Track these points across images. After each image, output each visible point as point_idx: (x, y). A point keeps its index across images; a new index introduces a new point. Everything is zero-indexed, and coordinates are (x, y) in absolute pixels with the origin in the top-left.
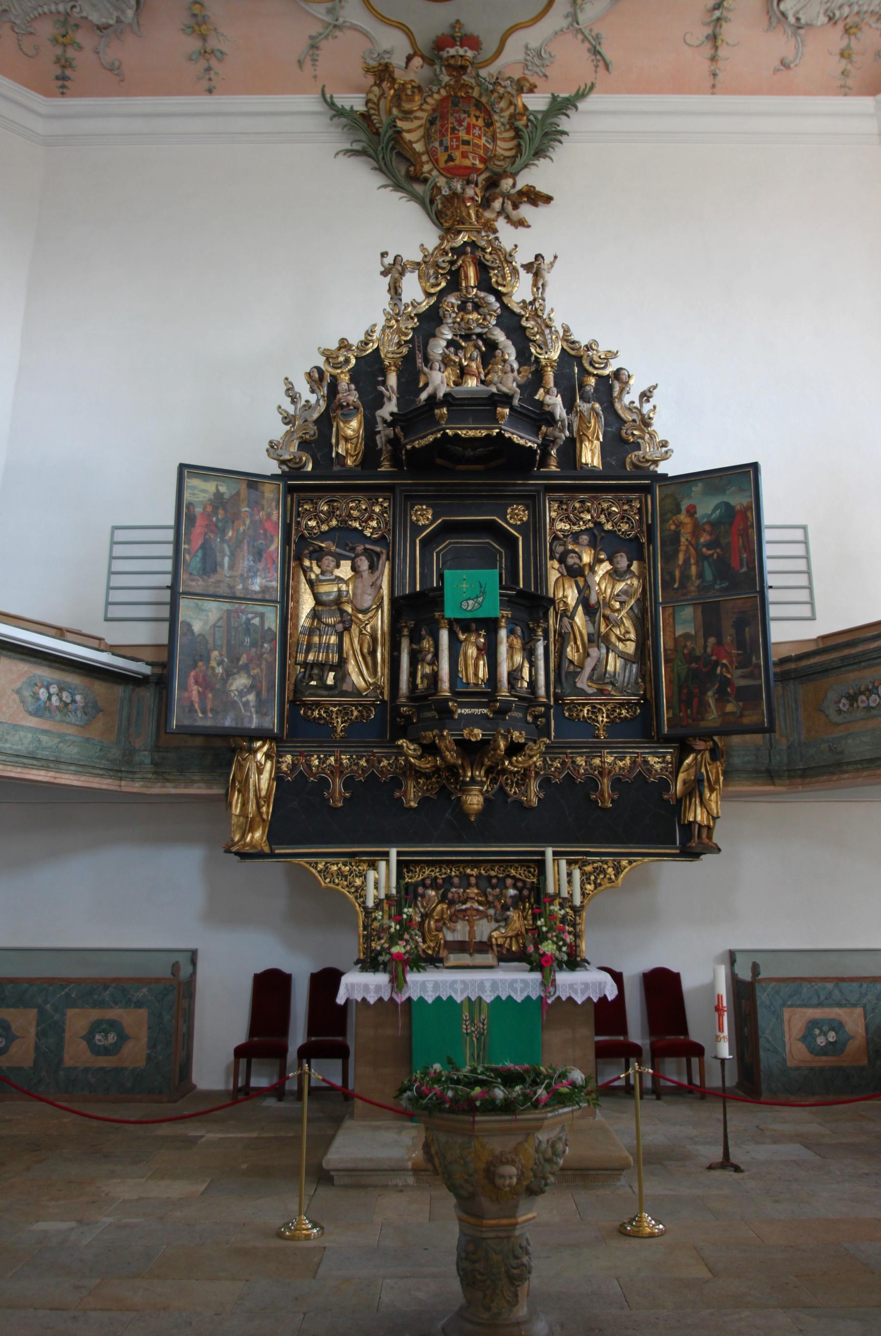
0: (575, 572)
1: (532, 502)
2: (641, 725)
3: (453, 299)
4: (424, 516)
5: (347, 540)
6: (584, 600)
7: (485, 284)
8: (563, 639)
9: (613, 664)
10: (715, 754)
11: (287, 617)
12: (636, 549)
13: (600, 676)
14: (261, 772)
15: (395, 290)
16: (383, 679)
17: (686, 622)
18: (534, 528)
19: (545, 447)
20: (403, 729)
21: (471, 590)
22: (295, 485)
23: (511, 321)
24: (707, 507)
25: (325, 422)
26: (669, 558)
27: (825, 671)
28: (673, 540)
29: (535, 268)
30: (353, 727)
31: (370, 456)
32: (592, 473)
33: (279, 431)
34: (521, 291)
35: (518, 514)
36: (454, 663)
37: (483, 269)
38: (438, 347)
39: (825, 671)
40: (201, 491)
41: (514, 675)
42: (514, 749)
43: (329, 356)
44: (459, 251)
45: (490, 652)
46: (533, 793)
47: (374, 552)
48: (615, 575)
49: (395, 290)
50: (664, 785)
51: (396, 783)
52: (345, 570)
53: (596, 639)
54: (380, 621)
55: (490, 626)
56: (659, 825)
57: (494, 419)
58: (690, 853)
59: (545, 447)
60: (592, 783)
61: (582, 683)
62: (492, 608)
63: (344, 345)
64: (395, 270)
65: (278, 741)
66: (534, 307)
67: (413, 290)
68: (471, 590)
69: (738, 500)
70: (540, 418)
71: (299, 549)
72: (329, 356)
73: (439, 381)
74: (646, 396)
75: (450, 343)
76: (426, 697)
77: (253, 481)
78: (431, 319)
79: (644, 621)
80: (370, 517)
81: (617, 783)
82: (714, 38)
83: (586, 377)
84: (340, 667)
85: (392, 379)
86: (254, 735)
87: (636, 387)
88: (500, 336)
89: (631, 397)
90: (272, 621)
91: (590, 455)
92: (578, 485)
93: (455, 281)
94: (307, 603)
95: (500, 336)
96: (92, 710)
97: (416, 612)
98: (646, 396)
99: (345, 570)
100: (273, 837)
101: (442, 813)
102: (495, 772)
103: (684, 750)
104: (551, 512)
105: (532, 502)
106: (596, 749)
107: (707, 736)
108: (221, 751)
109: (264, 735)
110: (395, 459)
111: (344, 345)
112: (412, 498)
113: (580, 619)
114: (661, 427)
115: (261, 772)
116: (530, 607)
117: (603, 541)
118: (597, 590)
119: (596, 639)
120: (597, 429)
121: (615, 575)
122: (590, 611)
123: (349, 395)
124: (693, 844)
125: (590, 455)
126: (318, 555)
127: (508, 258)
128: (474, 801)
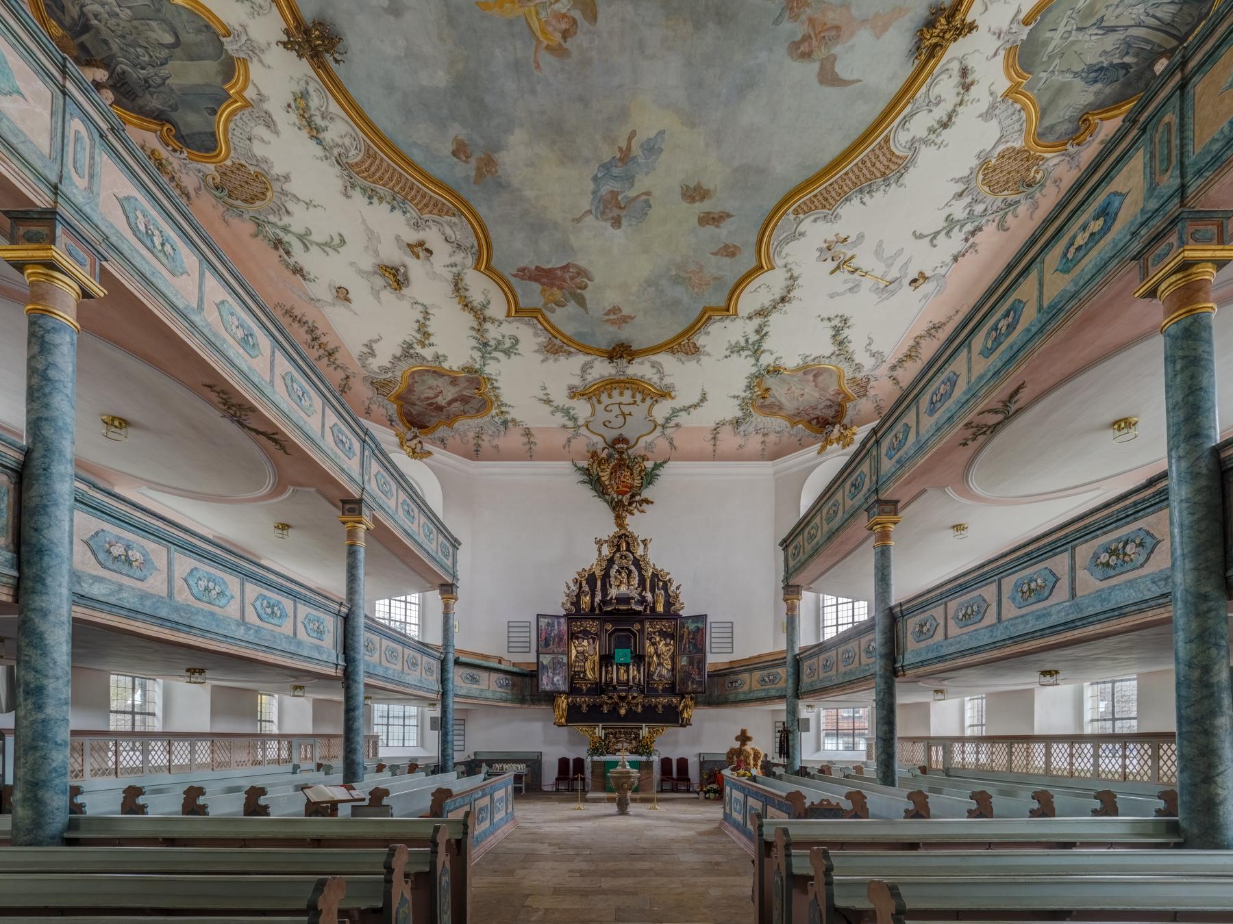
0: (654, 644)
1: (641, 622)
2: (671, 690)
3: (618, 555)
4: (609, 627)
5: (586, 634)
6: (656, 652)
7: (628, 549)
8: (650, 664)
9: (664, 672)
10: (692, 699)
11: (569, 657)
12: (672, 636)
13: (660, 675)
14: (563, 702)
15: (600, 551)
16: (597, 675)
17: (684, 661)
18: (641, 631)
19: (645, 609)
20: (603, 691)
21: (622, 655)
22: (569, 617)
23: (636, 562)
24: (692, 627)
25: (578, 596)
26: (681, 641)
27: (725, 675)
28: (682, 636)
29: (644, 541)
30: (588, 690)
31: (592, 608)
32: (660, 614)
33: (564, 599)
34: (640, 551)
35: (637, 626)
36: (616, 674)
37: (628, 544)
38: (613, 572)
39: (725, 675)
40: (543, 622)
41: (634, 678)
42: (634, 698)
43: (578, 574)
44: (620, 537)
45: (627, 671)
46: (640, 710)
47: (593, 637)
48: (666, 645)
49: (600, 551)
50: (677, 707)
51: (601, 706)
52: (585, 643)
53: (660, 664)
54: (597, 658)
55: (628, 665)
56: (673, 717)
57: (629, 603)
58: (682, 726)
59: (645, 609)
60: (656, 706)
61: (655, 677)
62: (629, 660)
63: (584, 570)
64: (599, 543)
65: (568, 694)
66: (644, 557)
67: (606, 551)
68: (622, 655)
69: (700, 626)
70: (643, 601)
71: (573, 636)
72: (578, 574)
73: (613, 592)
74: (678, 588)
75: (618, 571)
76: (609, 684)
77: (558, 617)
78: (611, 561)
79: (673, 658)
80: (593, 626)
81: (663, 706)
82: (714, 438)
83: (658, 581)
84: (585, 672)
85: (599, 583)
86: (560, 693)
87: (675, 585)
88: (632, 568)
89: (673, 588)
90: (565, 660)
91: (660, 608)
92: (655, 617)
93: (618, 550)
94: (574, 652)
95: (632, 568)
96: (514, 685)
97: (606, 660)
98: (678, 588)
99: (585, 643)
100: (567, 721)
101: (613, 714)
102: (628, 703)
103: (683, 697)
104: (647, 625)
105: (641, 622)
106: (657, 696)
107: (689, 693)
108: (550, 698)
109: (564, 692)
110: (600, 609)
111: (584, 570)
112: (605, 621)
113: (655, 658)
114: (682, 599)
115: (563, 702)
116: (639, 658)
117: (663, 634)
118: (660, 650)
119: (660, 664)
120: (662, 599)
121: (666, 645)
122: (658, 656)
123: (586, 588)
124: (685, 723)
125: (660, 608)
126: (577, 638)
127: (635, 539)
128: (623, 712)
